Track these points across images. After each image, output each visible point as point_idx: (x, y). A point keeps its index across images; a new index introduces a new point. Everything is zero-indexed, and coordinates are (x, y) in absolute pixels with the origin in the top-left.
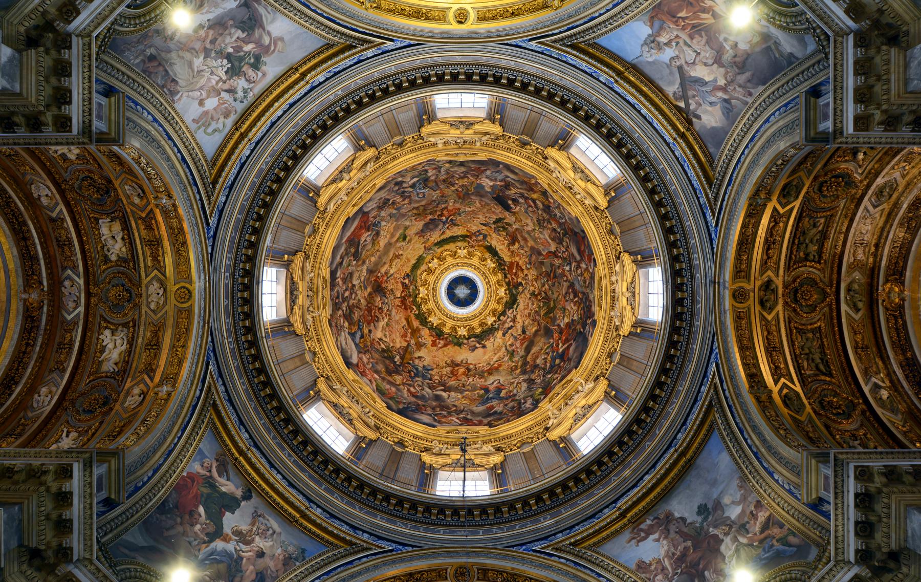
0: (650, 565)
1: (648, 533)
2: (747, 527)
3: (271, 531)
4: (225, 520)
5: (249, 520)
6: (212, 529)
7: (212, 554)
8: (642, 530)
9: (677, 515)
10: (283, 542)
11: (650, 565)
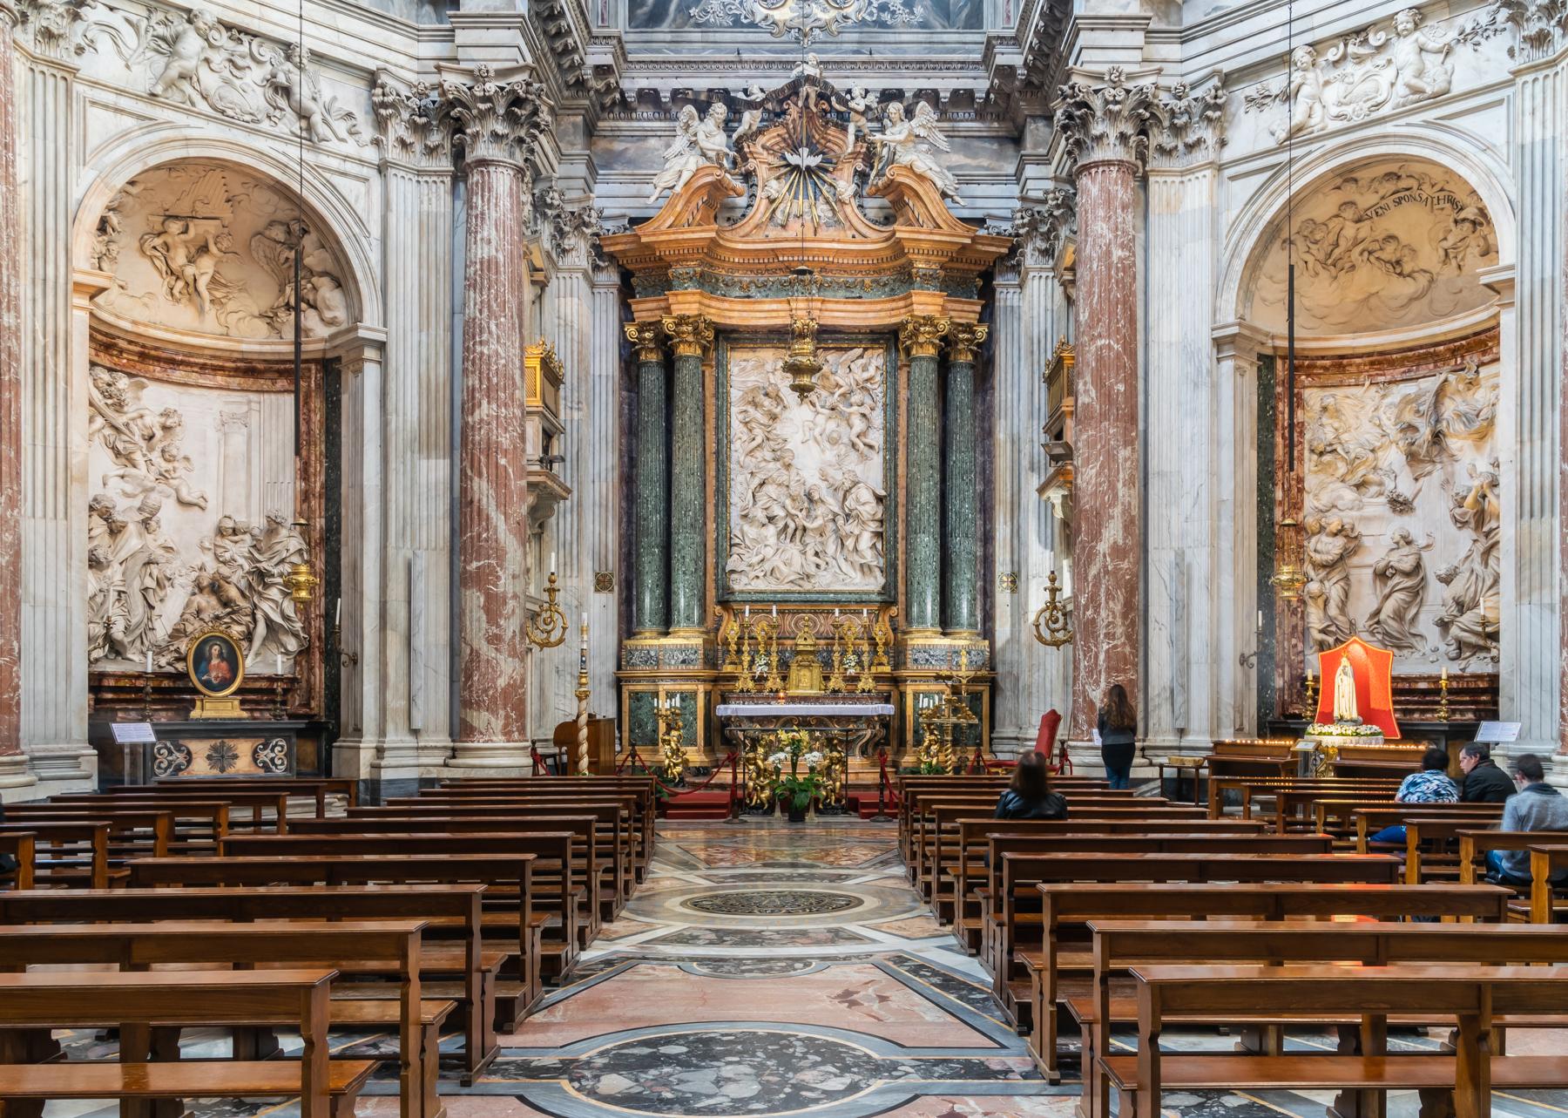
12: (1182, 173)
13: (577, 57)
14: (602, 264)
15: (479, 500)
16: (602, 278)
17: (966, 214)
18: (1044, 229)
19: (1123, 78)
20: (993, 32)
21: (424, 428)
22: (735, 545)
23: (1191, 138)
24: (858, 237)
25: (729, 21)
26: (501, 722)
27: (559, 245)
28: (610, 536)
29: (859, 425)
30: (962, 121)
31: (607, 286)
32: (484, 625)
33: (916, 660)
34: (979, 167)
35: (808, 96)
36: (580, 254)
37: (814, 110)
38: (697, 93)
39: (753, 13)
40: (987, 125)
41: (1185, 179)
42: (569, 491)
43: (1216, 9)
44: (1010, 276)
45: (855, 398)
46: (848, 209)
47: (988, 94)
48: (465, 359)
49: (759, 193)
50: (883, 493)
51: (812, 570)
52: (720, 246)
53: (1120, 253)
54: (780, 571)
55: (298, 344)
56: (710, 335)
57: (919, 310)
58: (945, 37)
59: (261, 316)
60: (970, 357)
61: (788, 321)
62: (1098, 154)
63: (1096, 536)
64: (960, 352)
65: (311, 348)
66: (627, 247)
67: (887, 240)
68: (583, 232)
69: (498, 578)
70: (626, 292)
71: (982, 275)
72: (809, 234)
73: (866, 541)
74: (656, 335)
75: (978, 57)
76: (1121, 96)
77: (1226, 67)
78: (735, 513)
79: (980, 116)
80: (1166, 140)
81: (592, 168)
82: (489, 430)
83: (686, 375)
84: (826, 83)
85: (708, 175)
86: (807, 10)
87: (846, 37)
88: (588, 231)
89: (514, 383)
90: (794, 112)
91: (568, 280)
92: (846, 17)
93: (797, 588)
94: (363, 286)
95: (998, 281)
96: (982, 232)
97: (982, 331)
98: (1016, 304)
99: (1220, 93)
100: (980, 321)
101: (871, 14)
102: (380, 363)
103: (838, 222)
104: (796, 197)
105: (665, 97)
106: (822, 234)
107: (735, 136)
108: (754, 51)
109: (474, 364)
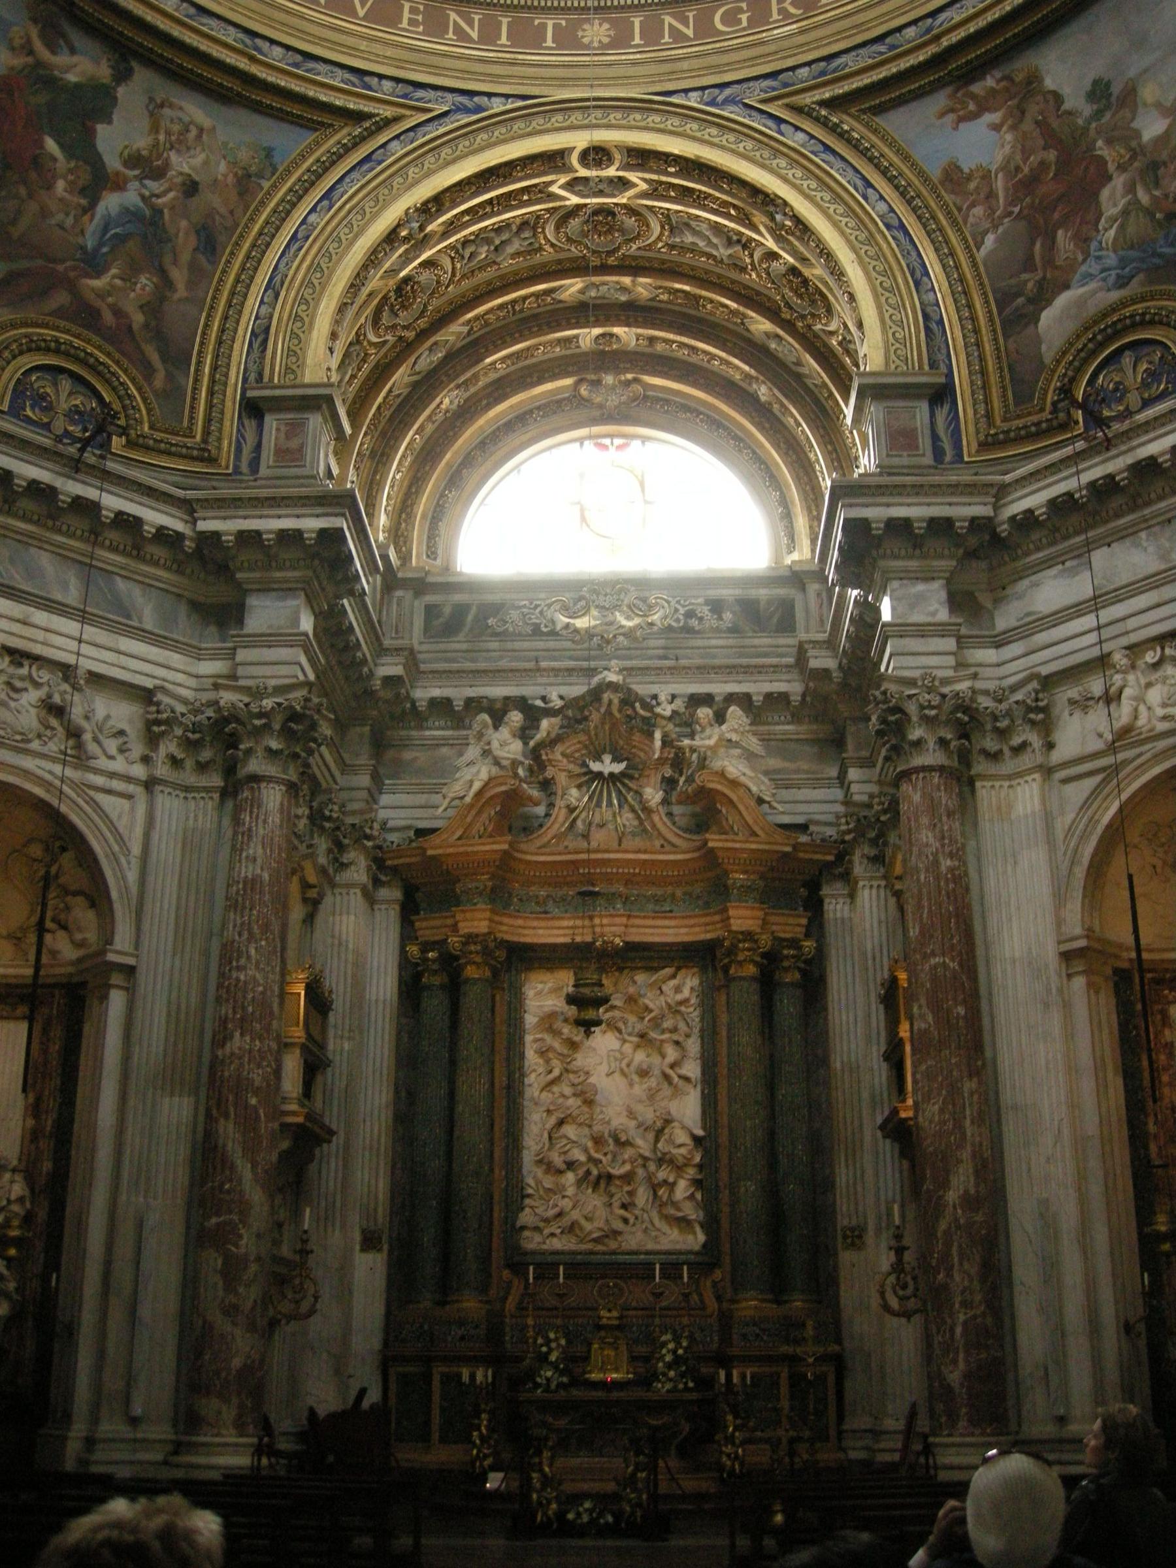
0: (969, 178)
1: (982, 109)
2: (1161, 171)
3: (194, 132)
4: (101, 146)
5: (146, 123)
6: (85, 177)
7: (106, 229)
8: (973, 97)
9: (1049, 83)
10: (225, 144)
11: (969, 178)
12: (1010, 777)
13: (366, 669)
14: (383, 878)
15: (224, 1146)
16: (384, 893)
17: (786, 820)
18: (872, 834)
19: (937, 683)
20: (803, 636)
21: (169, 1060)
22: (529, 1196)
23: (1016, 741)
24: (668, 848)
25: (529, 630)
26: (234, 1412)
27: (336, 860)
28: (381, 1185)
29: (672, 1054)
30: (778, 724)
31: (388, 902)
32: (221, 1293)
34: (797, 771)
35: (610, 702)
36: (359, 871)
37: (617, 715)
38: (492, 701)
39: (553, 622)
40: (803, 728)
41: (1014, 783)
42: (332, 1133)
43: (1028, 614)
44: (839, 885)
45: (668, 1024)
46: (656, 818)
47: (804, 695)
48: (220, 986)
49: (560, 803)
50: (700, 1132)
51: (618, 1225)
52: (515, 859)
53: (949, 863)
54: (581, 1228)
55: (37, 967)
56: (501, 954)
57: (737, 925)
58: (756, 642)
59: (9, 936)
60: (797, 976)
61: (589, 939)
62: (918, 761)
63: (945, 1185)
64: (787, 969)
65: (54, 971)
66: (413, 860)
67: (699, 849)
68: (365, 847)
69: (240, 1237)
70: (409, 909)
72: (615, 845)
73: (682, 1189)
74: (441, 955)
75: (791, 660)
76: (936, 700)
77: (1045, 671)
78: (528, 1157)
79: (796, 718)
80: (990, 744)
81: (376, 777)
82: (242, 1065)
83: (472, 998)
84: (629, 690)
85: (501, 784)
86: (610, 618)
87: (652, 643)
88: (370, 844)
89: (272, 1013)
90: (595, 717)
92: (652, 624)
93: (600, 1248)
94: (117, 906)
95: (826, 891)
96: (804, 839)
97: (809, 945)
99: (1041, 696)
100: (807, 935)
101: (678, 620)
102: (127, 989)
103: (645, 830)
104: (599, 805)
105: (458, 705)
106: (628, 843)
107: (532, 743)
108: (555, 659)
109: (228, 992)
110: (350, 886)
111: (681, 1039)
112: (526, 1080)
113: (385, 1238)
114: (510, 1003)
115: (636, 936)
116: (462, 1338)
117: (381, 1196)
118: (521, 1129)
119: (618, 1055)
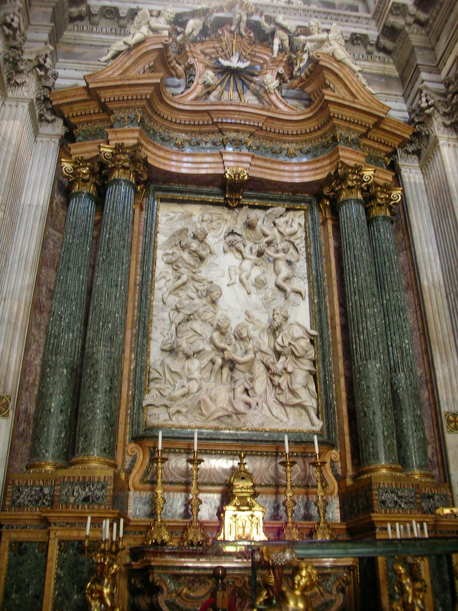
29: (285, 271)
31: (50, 136)
33: (383, 502)
46: (273, 98)
49: (196, 80)
51: (241, 407)
54: (207, 408)
61: (221, 172)
71: (389, 155)
91: (15, 109)
98: (418, 182)
105: (123, 13)
110: (18, 100)
111: (293, 259)
112: (157, 285)
113: (12, 405)
114: (146, 221)
115: (258, 174)
116: (86, 499)
117: (12, 368)
118: (151, 321)
119: (238, 271)
